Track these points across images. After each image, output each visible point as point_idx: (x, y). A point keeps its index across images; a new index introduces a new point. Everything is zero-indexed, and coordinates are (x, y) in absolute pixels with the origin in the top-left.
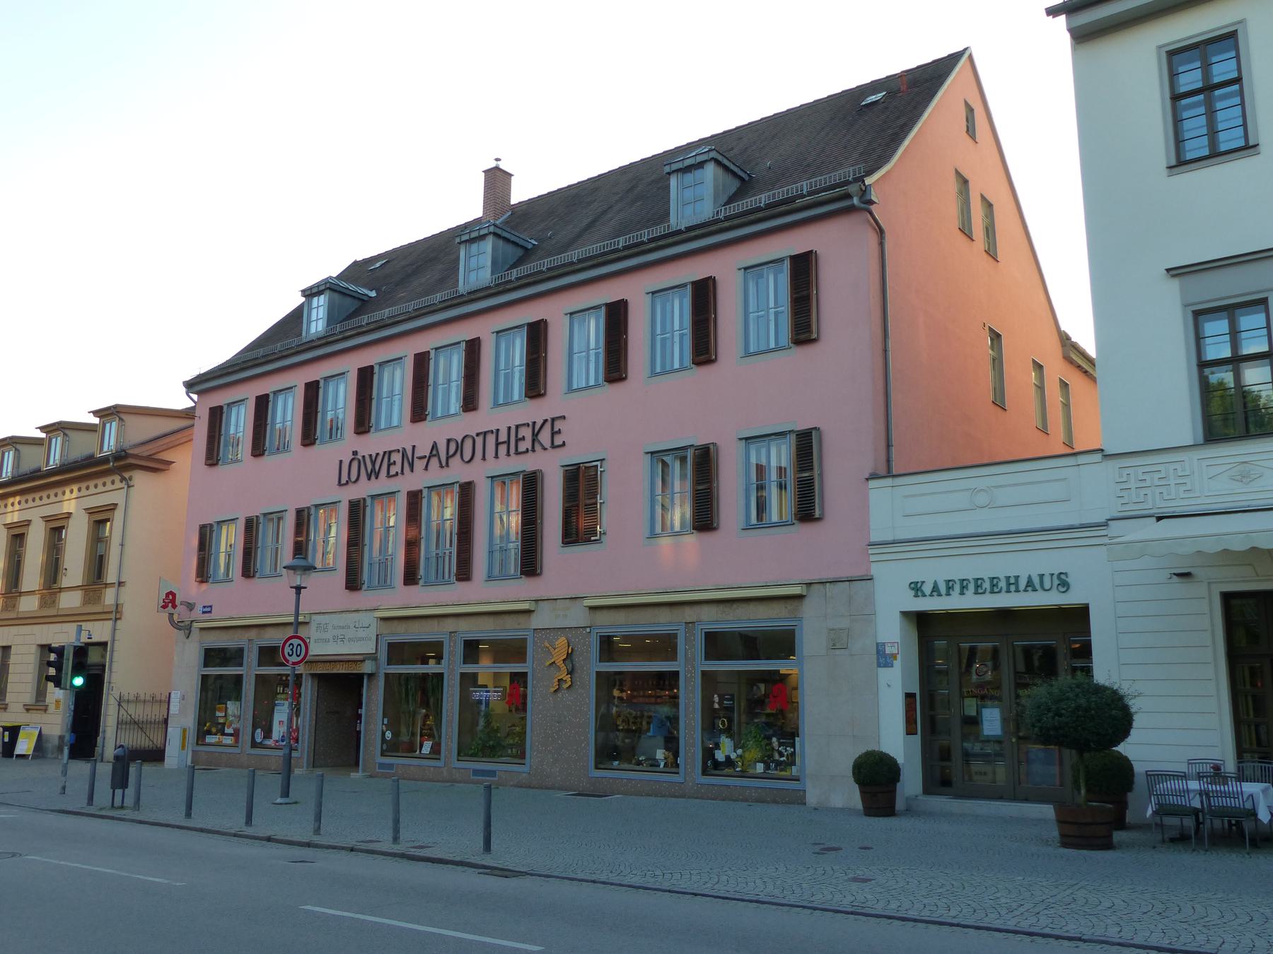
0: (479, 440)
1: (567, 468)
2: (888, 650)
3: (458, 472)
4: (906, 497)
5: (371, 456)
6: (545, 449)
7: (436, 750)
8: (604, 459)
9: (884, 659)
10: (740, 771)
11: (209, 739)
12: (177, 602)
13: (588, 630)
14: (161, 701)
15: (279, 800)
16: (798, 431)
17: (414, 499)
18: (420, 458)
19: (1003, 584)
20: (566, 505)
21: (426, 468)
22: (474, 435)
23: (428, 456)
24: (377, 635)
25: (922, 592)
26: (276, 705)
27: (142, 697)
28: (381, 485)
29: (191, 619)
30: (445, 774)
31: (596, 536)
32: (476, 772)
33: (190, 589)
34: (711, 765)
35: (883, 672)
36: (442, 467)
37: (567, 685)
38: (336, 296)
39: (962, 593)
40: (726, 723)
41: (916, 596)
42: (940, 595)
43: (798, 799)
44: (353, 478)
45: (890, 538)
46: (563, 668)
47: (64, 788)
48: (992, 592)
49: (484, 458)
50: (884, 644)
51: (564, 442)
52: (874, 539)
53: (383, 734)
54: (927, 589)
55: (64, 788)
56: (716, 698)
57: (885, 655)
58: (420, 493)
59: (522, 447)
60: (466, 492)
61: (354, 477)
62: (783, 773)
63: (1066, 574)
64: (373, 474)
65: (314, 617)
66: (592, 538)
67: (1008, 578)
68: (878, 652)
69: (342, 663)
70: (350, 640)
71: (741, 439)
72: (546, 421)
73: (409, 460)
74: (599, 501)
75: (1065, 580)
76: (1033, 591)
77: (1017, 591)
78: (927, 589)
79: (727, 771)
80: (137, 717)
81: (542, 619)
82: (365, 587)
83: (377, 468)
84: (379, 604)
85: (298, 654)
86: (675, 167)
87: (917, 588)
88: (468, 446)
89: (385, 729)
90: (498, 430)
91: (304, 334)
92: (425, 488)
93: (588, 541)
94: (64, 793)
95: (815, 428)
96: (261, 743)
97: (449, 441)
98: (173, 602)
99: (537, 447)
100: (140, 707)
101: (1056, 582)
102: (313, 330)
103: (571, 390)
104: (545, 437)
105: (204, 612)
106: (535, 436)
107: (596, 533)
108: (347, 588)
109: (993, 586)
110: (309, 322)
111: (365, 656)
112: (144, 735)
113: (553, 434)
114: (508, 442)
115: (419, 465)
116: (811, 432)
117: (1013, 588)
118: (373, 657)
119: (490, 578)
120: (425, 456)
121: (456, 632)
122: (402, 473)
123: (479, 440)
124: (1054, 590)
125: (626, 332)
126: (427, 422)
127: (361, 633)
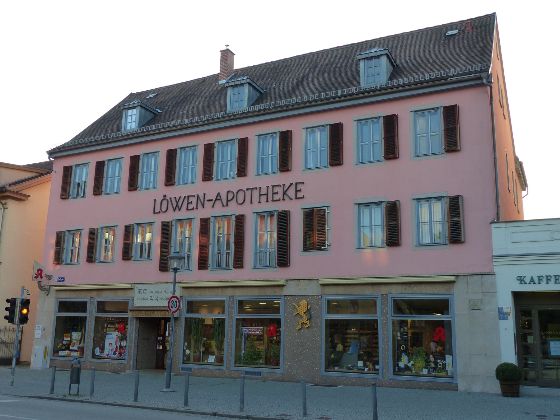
0: (248, 193)
2: (505, 311)
3: (234, 209)
5: (175, 198)
6: (291, 199)
7: (220, 360)
8: (329, 206)
10: (415, 373)
11: (62, 353)
12: (43, 275)
13: (320, 297)
17: (205, 224)
18: (208, 201)
20: (305, 230)
21: (213, 207)
22: (245, 190)
23: (214, 199)
25: (524, 281)
28: (183, 214)
30: (227, 373)
32: (247, 373)
33: (50, 267)
34: (398, 370)
35: (502, 322)
36: (223, 206)
37: (307, 326)
38: (143, 110)
41: (521, 283)
42: (534, 283)
43: (454, 387)
44: (164, 209)
46: (305, 317)
47: (13, 382)
49: (251, 203)
50: (502, 308)
51: (304, 196)
53: (184, 351)
54: (527, 280)
55: (13, 382)
56: (399, 334)
57: (503, 314)
59: (276, 197)
60: (240, 220)
61: (164, 209)
62: (441, 374)
64: (177, 208)
65: (136, 286)
66: (322, 248)
68: (499, 312)
69: (159, 312)
70: (162, 299)
71: (356, 204)
72: (291, 184)
73: (201, 201)
74: (326, 228)
78: (527, 280)
79: (406, 372)
80: (5, 339)
83: (180, 205)
85: (176, 302)
86: (363, 56)
87: (521, 280)
88: (241, 195)
89: (185, 348)
91: (123, 129)
93: (320, 249)
94: (13, 386)
96: (98, 356)
97: (228, 192)
99: (286, 198)
100: (7, 334)
102: (128, 127)
104: (291, 193)
105: (58, 281)
106: (284, 193)
107: (325, 245)
108: (160, 270)
110: (126, 123)
112: (8, 350)
114: (267, 195)
115: (208, 205)
119: (255, 267)
120: (212, 200)
122: (197, 208)
123: (248, 193)
125: (342, 141)
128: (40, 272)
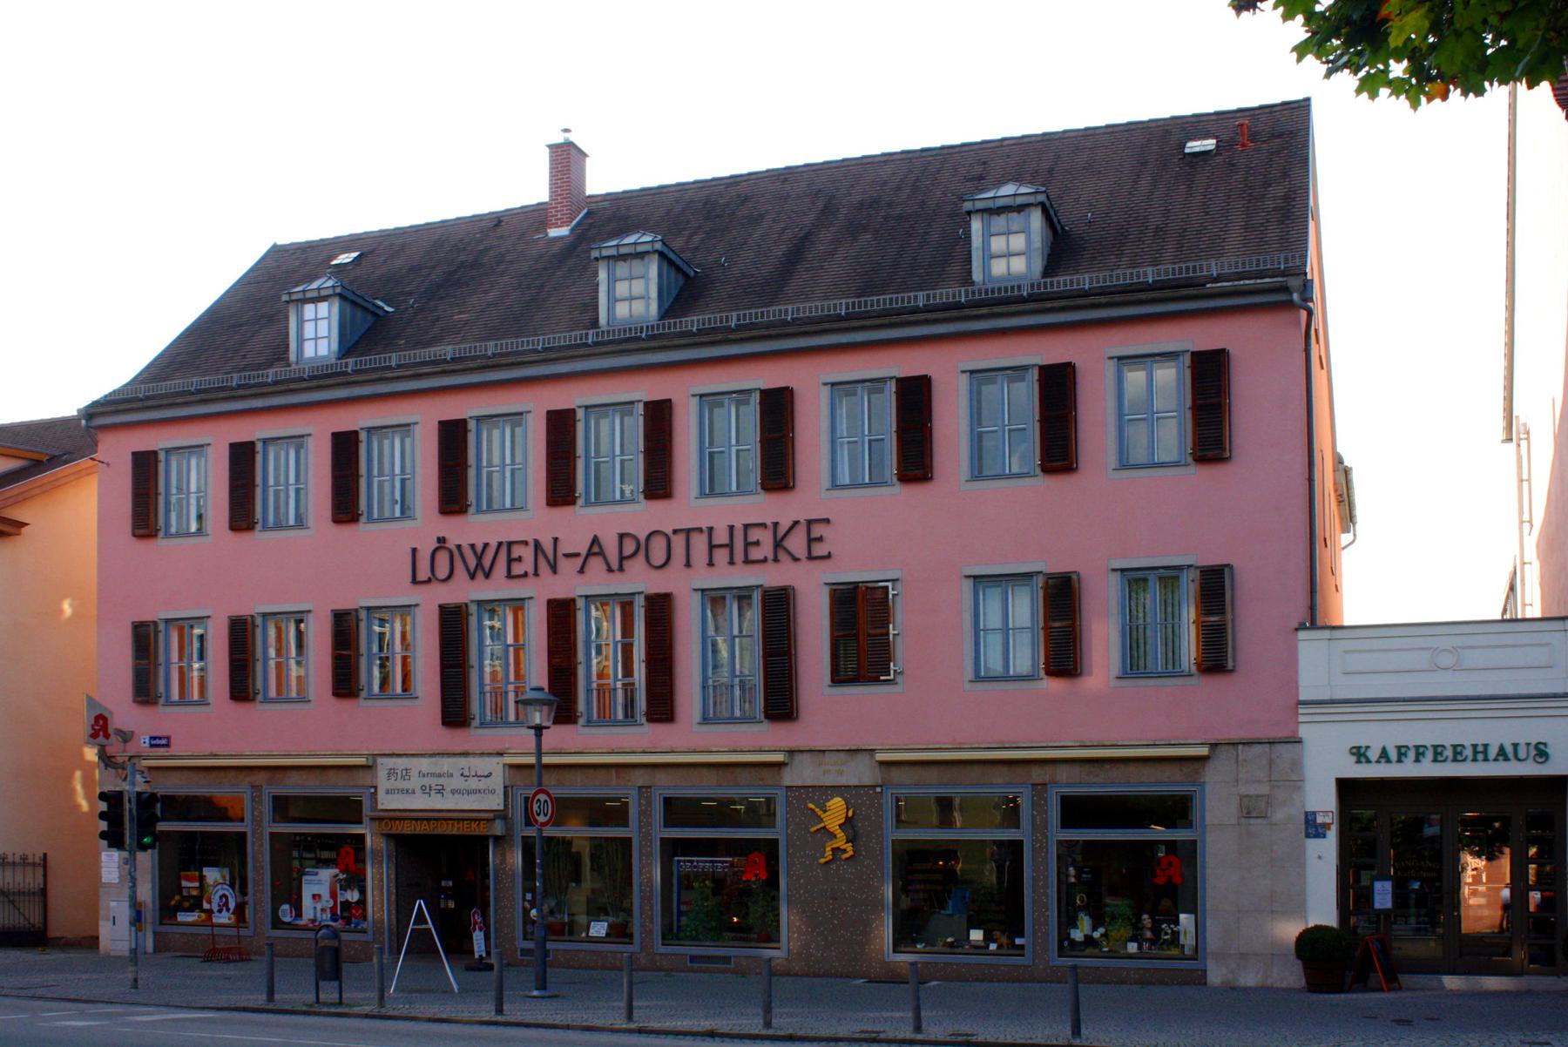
1: (835, 587)
2: (1320, 820)
4: (1346, 652)
5: (473, 546)
8: (897, 580)
9: (1313, 828)
12: (111, 731)
14: (14, 864)
15: (536, 993)
16: (1203, 567)
19: (1468, 752)
21: (582, 571)
24: (505, 787)
25: (1366, 757)
26: (305, 874)
27: (30, 860)
28: (496, 588)
29: (129, 754)
31: (889, 675)
35: (1313, 845)
36: (610, 570)
39: (1417, 760)
40: (1085, 900)
41: (1358, 762)
42: (1389, 761)
45: (1326, 697)
48: (1455, 760)
49: (688, 565)
50: (1314, 813)
51: (830, 553)
52: (1302, 697)
54: (1374, 754)
58: (572, 603)
63: (1545, 744)
65: (380, 760)
66: (882, 678)
67: (1475, 746)
68: (1307, 822)
69: (450, 822)
70: (453, 792)
72: (796, 523)
75: (1543, 751)
76: (1505, 760)
77: (1486, 759)
78: (1374, 754)
81: (803, 774)
82: (476, 723)
84: (507, 746)
87: (1359, 754)
90: (711, 529)
92: (581, 596)
95: (1228, 565)
98: (105, 728)
99: (782, 555)
101: (1533, 752)
102: (309, 351)
103: (835, 486)
105: (152, 746)
107: (889, 672)
108: (444, 723)
109: (1456, 753)
110: (301, 340)
111: (496, 813)
112: (17, 912)
113: (811, 541)
116: (1223, 570)
117: (1480, 757)
118: (502, 815)
119: (705, 720)
120: (578, 555)
121: (650, 787)
122: (536, 574)
123: (678, 543)
124: (1530, 760)
126: (577, 507)
127: (483, 784)
128: (101, 722)
